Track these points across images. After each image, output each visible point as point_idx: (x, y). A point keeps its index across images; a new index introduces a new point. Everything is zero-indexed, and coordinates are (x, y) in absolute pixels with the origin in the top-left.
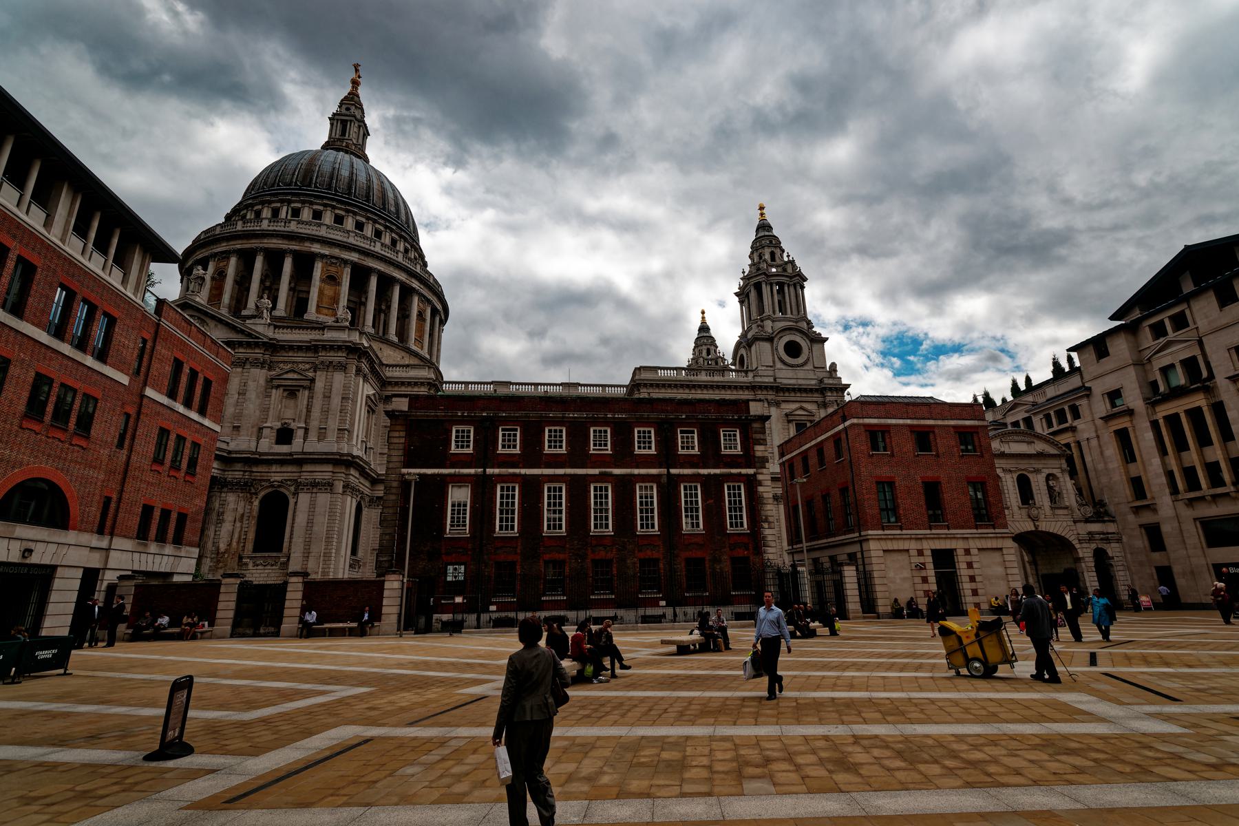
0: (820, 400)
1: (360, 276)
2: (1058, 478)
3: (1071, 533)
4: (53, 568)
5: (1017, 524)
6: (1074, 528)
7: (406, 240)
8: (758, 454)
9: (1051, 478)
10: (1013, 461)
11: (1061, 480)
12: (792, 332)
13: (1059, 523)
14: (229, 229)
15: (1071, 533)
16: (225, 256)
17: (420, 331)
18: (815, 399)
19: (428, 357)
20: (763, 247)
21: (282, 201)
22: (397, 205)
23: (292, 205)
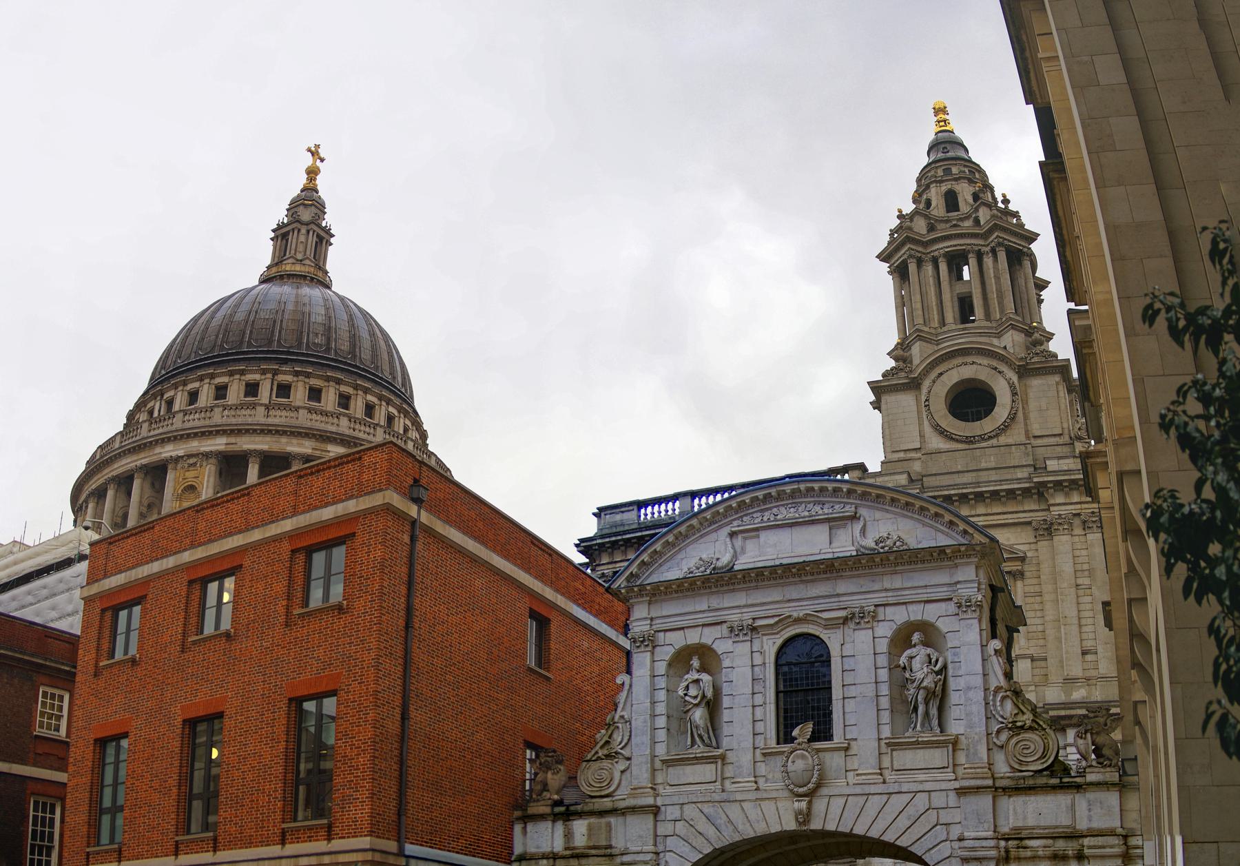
0: (1040, 516)
3: (940, 832)
5: (734, 811)
9: (916, 637)
10: (774, 595)
12: (969, 359)
13: (898, 802)
15: (940, 832)
18: (1023, 517)
20: (928, 187)
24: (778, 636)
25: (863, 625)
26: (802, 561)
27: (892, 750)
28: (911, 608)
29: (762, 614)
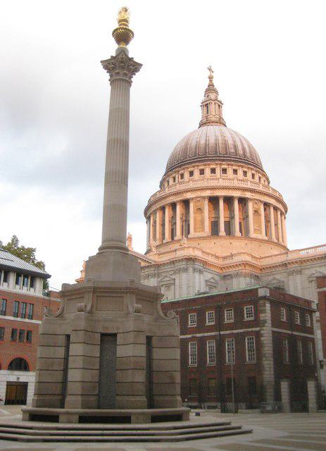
1: (214, 201)
4: (27, 383)
7: (242, 167)
8: (262, 319)
14: (163, 194)
16: (155, 212)
17: (258, 222)
19: (266, 238)
21: (175, 172)
22: (235, 147)
23: (180, 172)
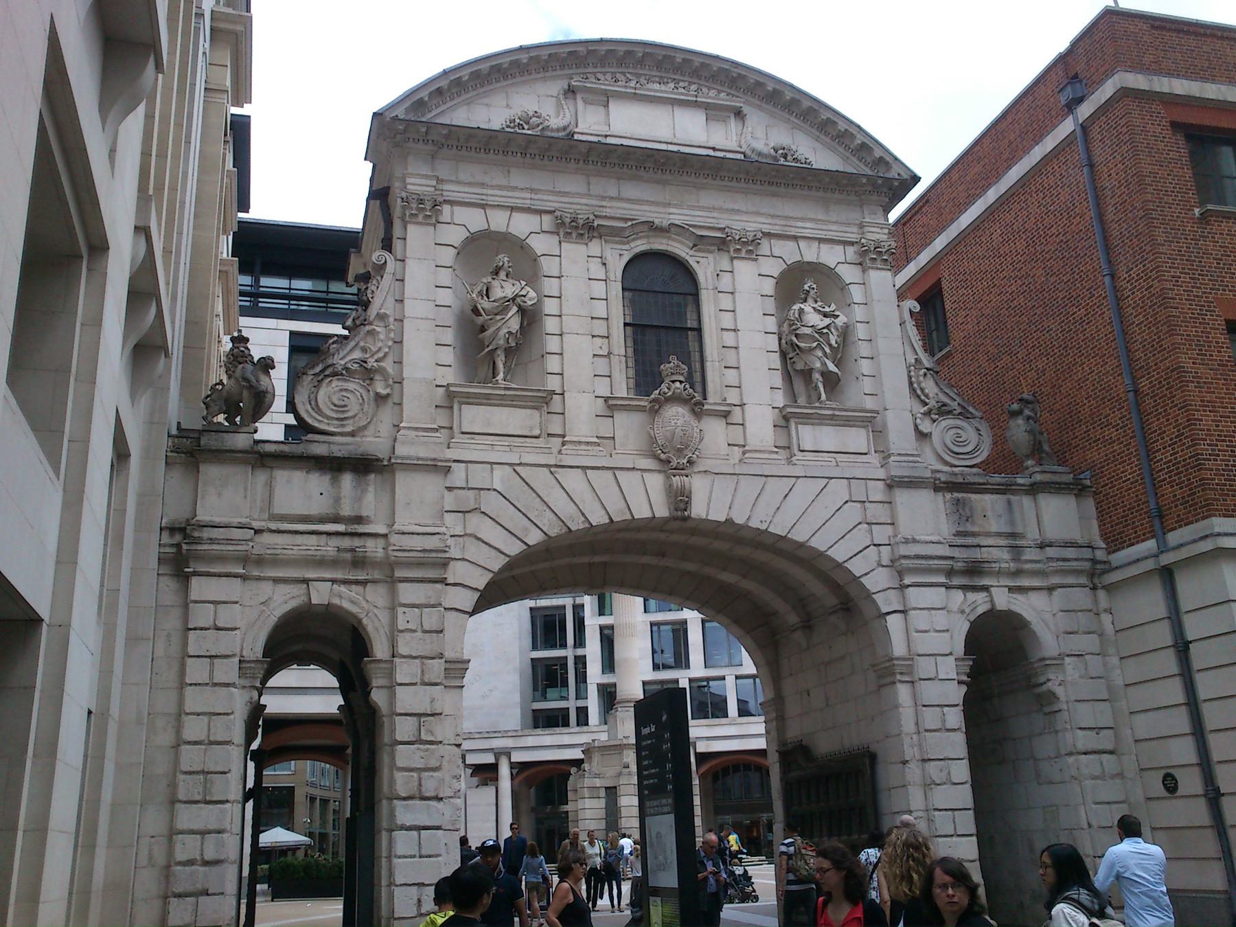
2: (843, 287)
5: (573, 480)
6: (879, 512)
11: (857, 294)
24: (627, 247)
25: (743, 254)
26: (676, 150)
27: (796, 424)
28: (802, 244)
29: (608, 212)
